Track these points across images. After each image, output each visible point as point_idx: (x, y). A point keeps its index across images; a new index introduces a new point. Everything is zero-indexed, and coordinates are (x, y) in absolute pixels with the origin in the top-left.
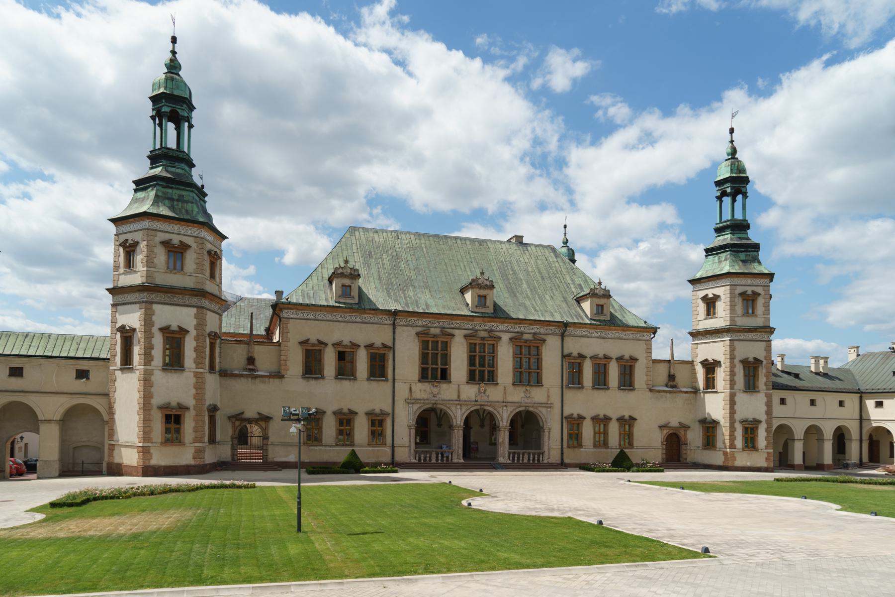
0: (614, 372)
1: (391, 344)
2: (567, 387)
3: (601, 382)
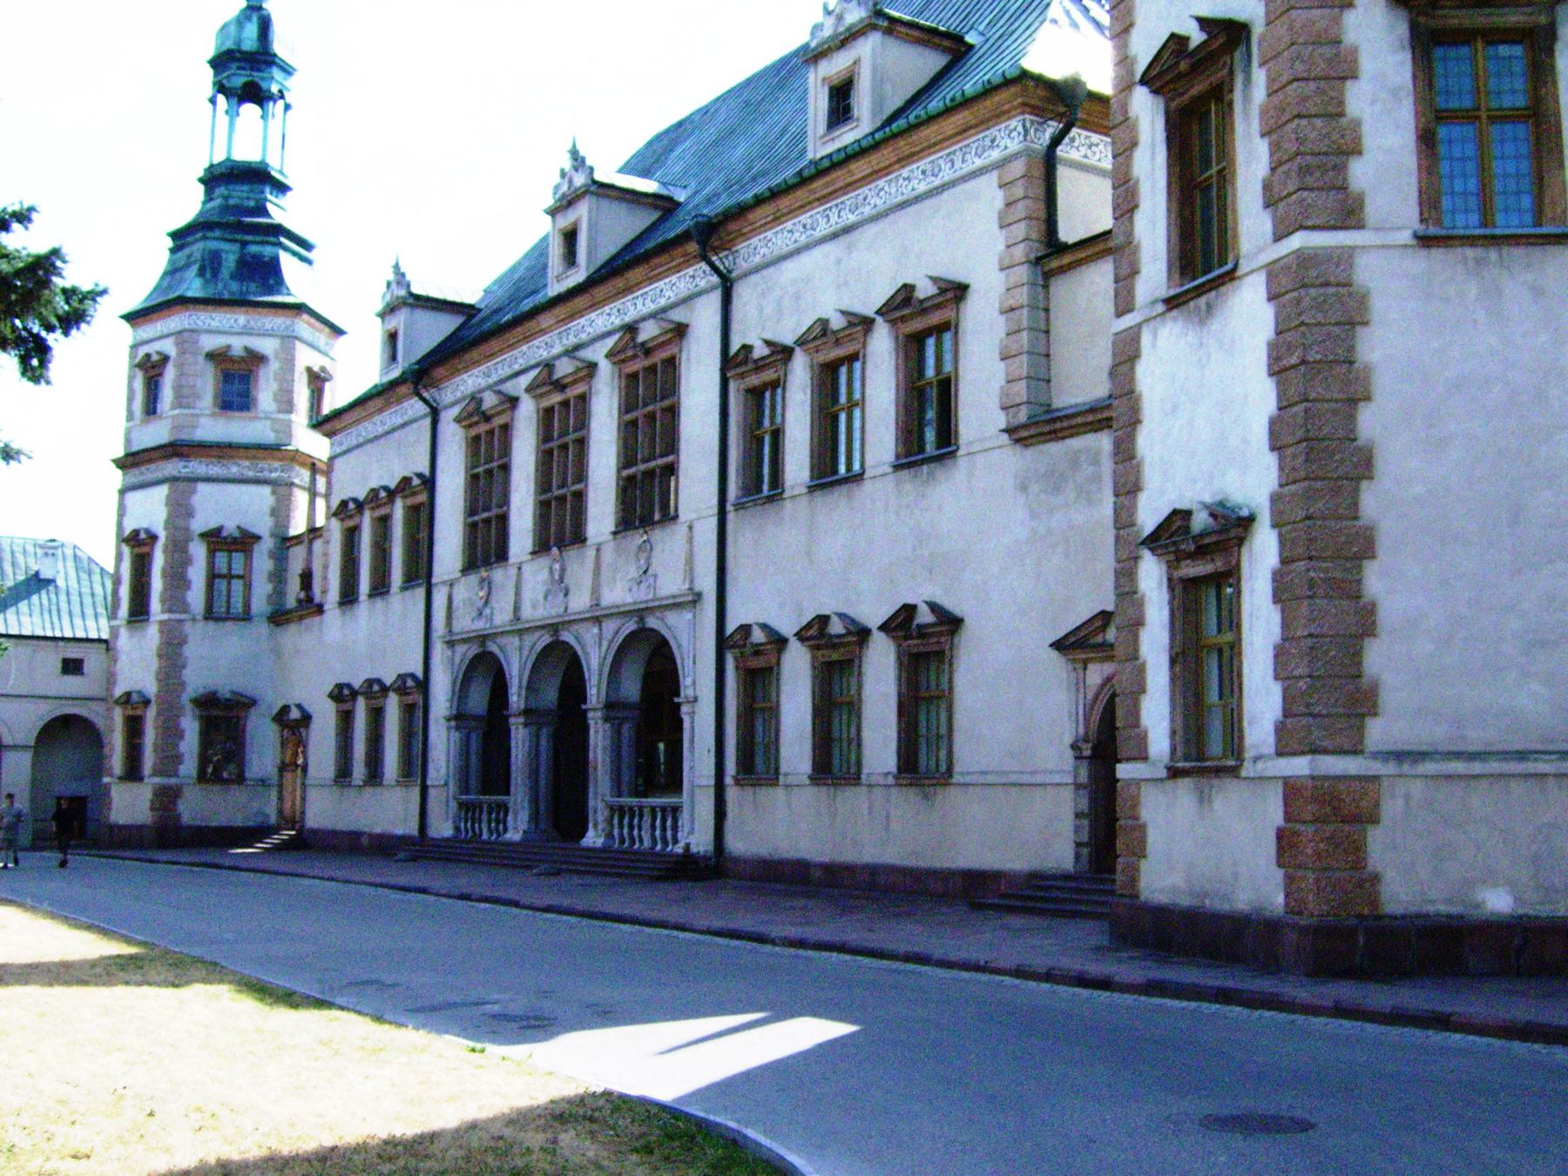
1: (427, 472)
2: (739, 506)
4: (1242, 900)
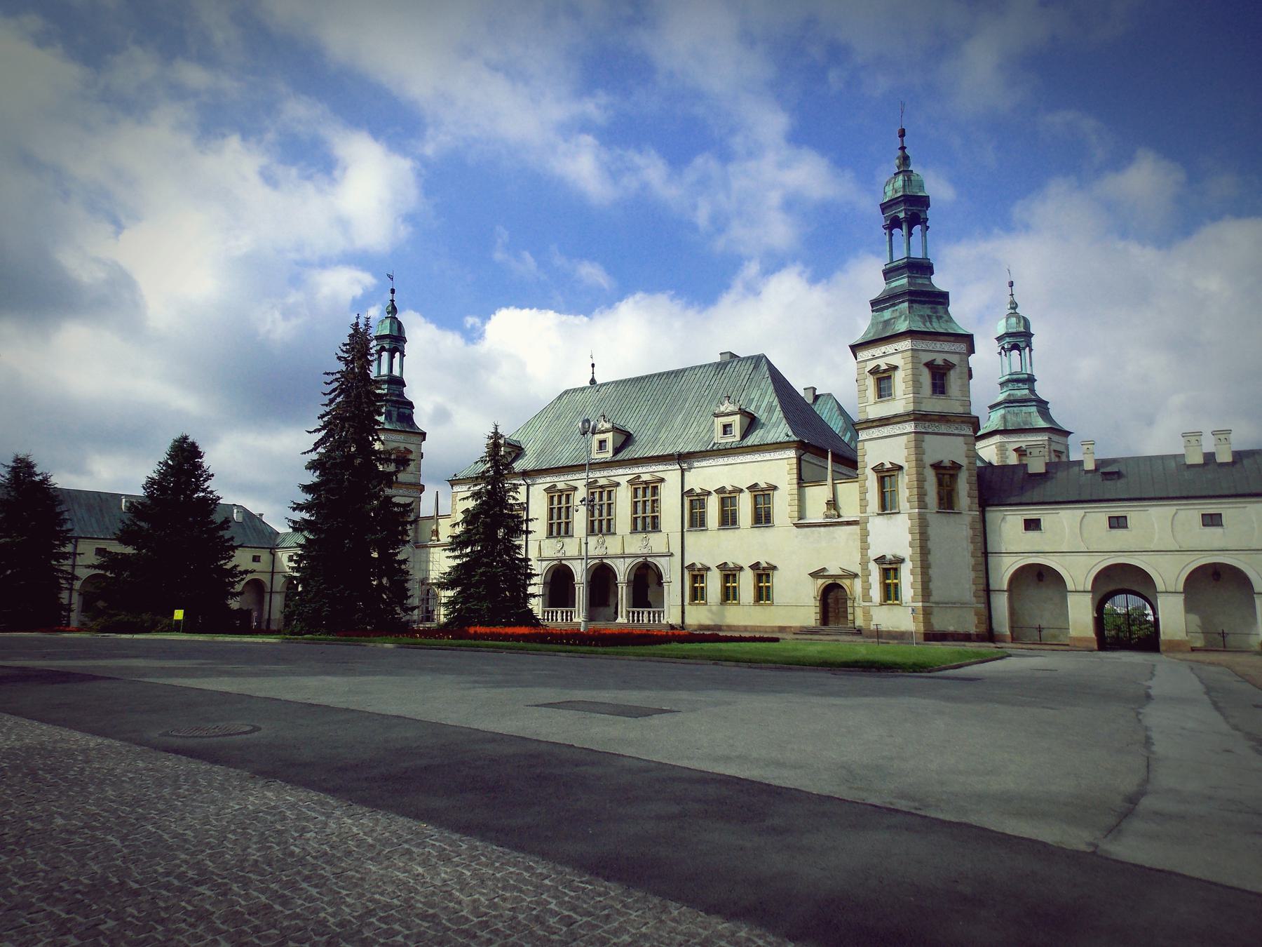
0: (745, 506)
3: (728, 519)
4: (903, 629)
